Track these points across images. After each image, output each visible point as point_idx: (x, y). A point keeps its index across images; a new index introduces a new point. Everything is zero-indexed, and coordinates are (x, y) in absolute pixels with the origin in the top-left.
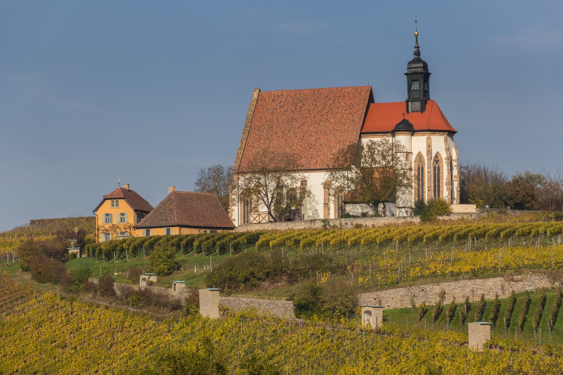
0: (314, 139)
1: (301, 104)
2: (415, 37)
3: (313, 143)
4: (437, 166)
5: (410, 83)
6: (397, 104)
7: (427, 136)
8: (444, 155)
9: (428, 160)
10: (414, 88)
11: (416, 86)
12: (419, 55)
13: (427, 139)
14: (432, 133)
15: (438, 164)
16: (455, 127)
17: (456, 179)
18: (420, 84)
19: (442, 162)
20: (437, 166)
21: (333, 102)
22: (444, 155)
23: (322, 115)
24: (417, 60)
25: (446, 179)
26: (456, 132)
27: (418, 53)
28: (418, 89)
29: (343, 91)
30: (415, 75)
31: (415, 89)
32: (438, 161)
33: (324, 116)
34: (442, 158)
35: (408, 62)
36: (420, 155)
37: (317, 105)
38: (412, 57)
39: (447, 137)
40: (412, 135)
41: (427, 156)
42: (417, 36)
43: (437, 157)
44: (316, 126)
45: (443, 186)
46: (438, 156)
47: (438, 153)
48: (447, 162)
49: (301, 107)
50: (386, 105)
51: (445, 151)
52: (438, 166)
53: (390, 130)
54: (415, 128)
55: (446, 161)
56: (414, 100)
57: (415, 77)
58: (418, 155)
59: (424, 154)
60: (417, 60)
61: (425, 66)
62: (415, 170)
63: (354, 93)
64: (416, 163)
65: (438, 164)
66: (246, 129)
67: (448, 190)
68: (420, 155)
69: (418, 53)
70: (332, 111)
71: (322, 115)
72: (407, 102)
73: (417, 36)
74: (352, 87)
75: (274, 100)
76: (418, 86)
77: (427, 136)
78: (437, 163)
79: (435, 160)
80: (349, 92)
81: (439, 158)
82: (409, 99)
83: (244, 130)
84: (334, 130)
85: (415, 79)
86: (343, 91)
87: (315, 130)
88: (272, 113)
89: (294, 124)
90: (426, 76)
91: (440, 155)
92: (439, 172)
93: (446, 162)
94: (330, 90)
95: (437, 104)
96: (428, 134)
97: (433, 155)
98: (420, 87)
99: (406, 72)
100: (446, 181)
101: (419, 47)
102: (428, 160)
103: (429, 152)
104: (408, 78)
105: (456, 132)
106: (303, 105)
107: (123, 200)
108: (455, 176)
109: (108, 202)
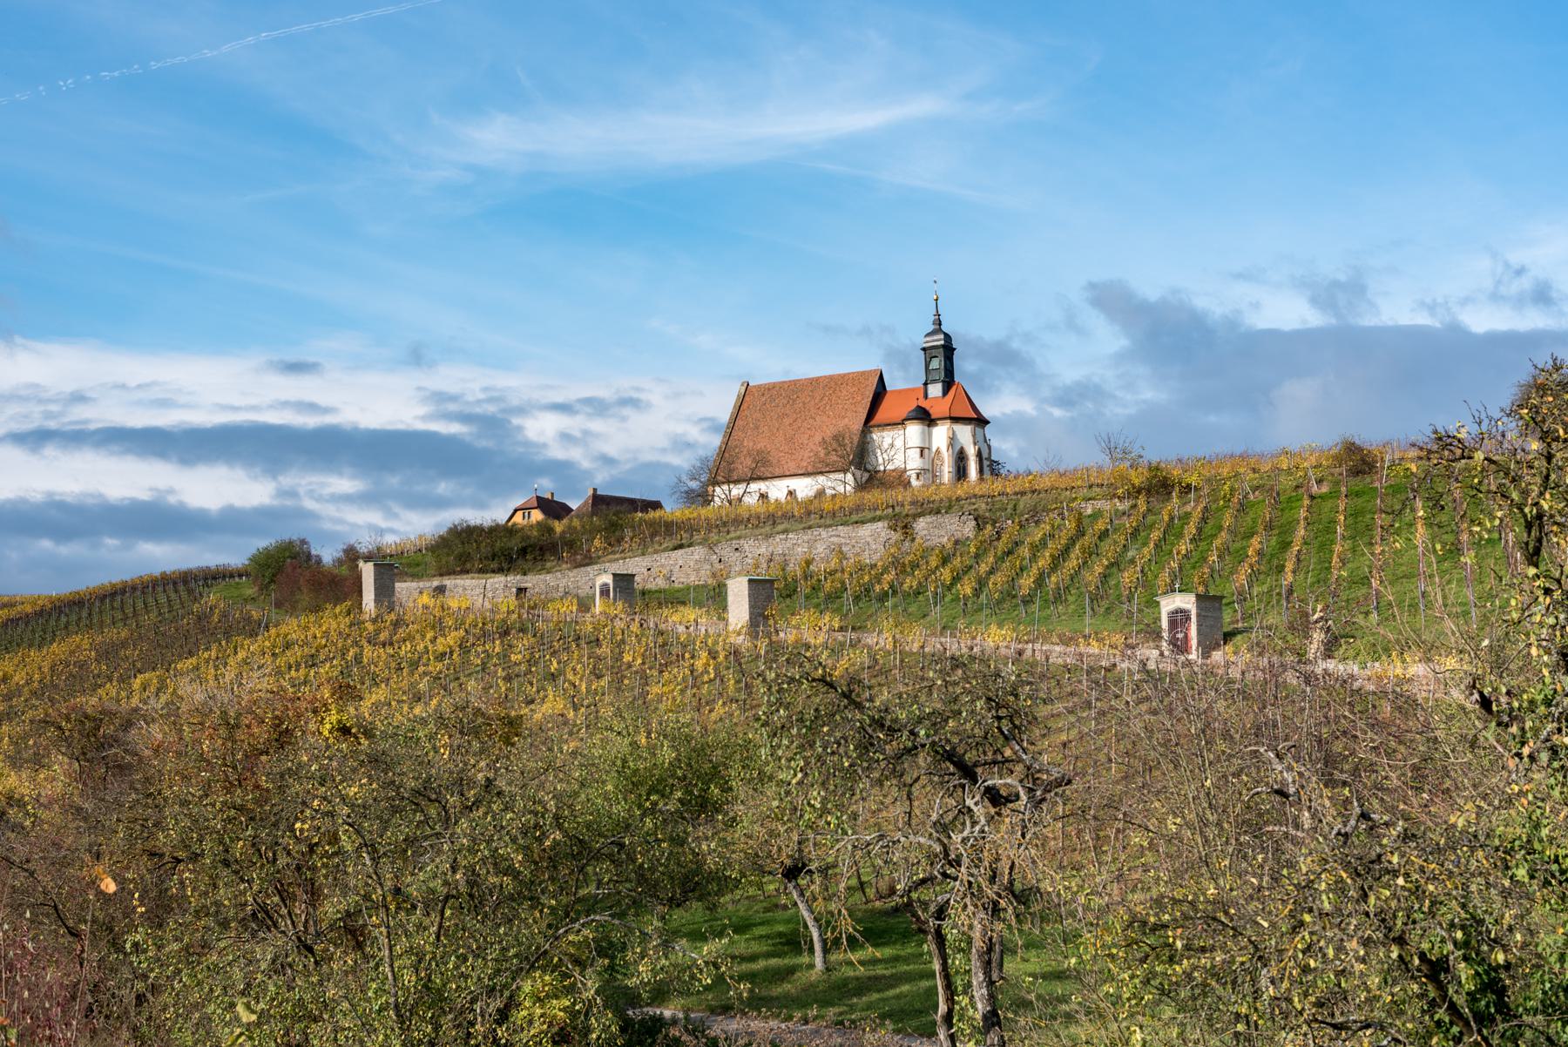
0: (807, 436)
6: (913, 390)
8: (971, 452)
11: (935, 364)
12: (940, 324)
13: (948, 429)
16: (986, 413)
22: (971, 452)
24: (938, 330)
26: (987, 422)
29: (846, 378)
38: (931, 328)
40: (929, 426)
44: (811, 421)
49: (794, 401)
50: (900, 392)
51: (972, 446)
54: (933, 417)
56: (934, 381)
57: (934, 352)
59: (944, 449)
60: (938, 330)
61: (947, 337)
68: (938, 451)
72: (926, 384)
86: (846, 378)
90: (948, 350)
94: (831, 378)
98: (940, 364)
109: (520, 514)
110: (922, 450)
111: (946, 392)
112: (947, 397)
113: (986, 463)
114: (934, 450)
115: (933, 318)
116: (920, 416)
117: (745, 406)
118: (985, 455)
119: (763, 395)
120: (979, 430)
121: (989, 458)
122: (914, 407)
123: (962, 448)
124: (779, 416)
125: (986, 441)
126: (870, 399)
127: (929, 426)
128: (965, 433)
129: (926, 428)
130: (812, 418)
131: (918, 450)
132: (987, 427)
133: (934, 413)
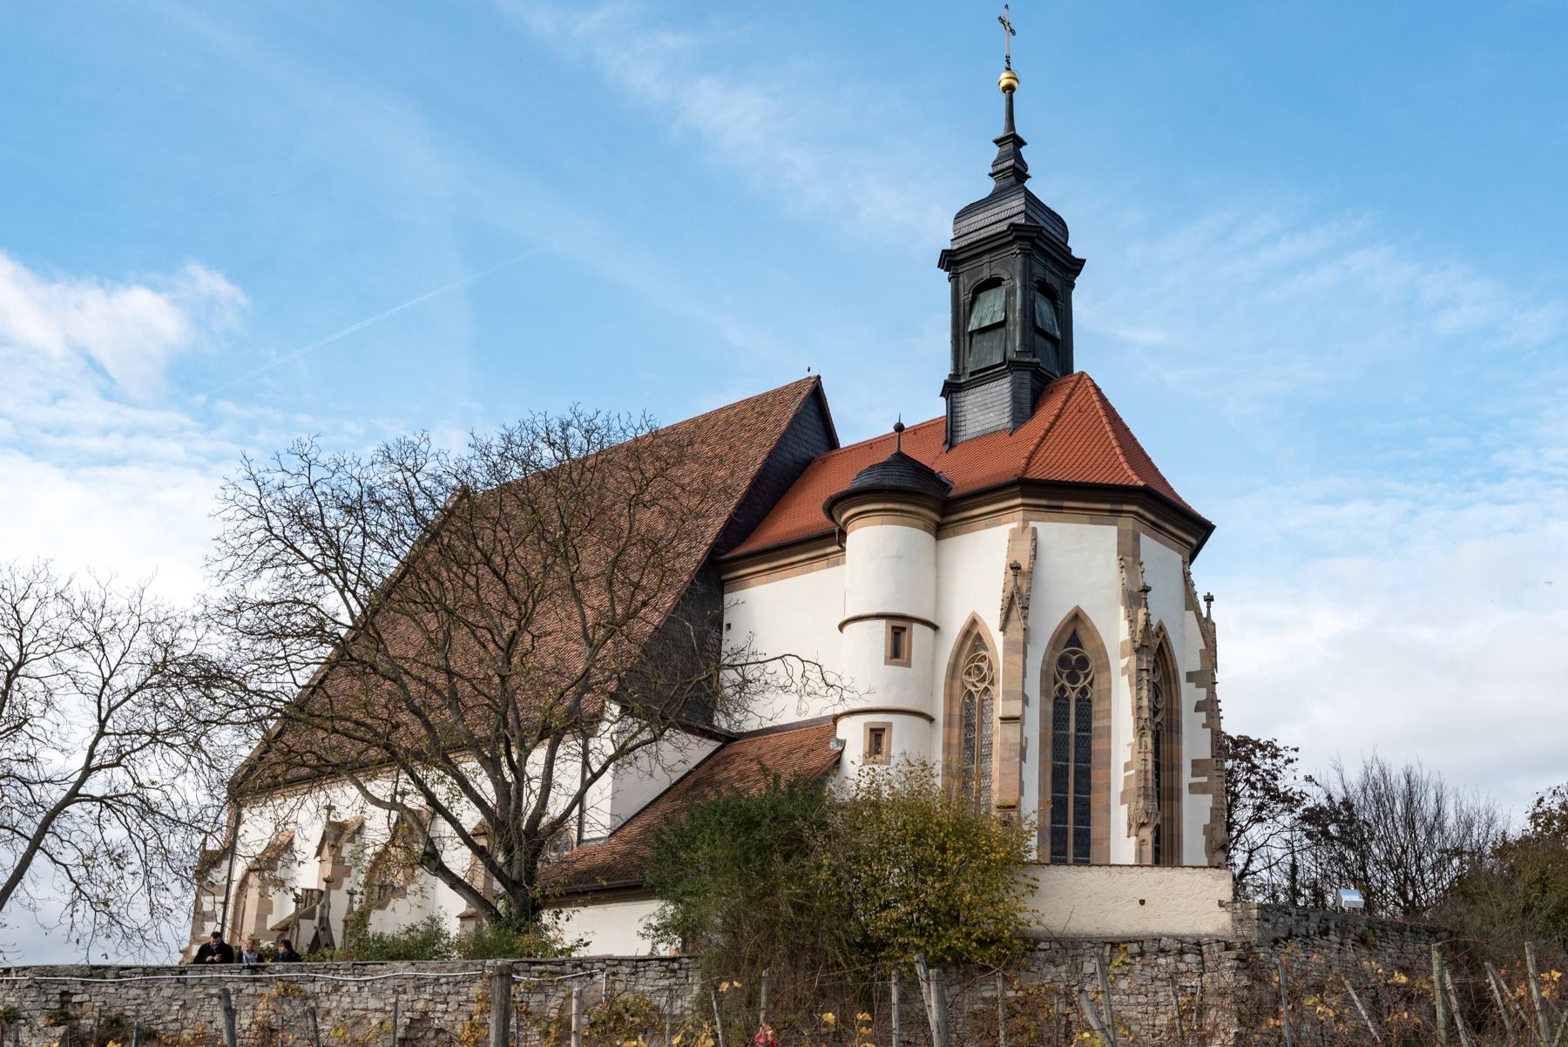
2: (1003, 97)
4: (1073, 696)
5: (962, 297)
7: (1015, 525)
9: (1008, 646)
10: (982, 319)
14: (1044, 502)
15: (1079, 685)
17: (1205, 779)
18: (1010, 293)
19: (1106, 667)
20: (1073, 696)
25: (1127, 767)
27: (1012, 173)
28: (999, 318)
31: (987, 323)
32: (1083, 662)
34: (1101, 650)
35: (958, 211)
36: (972, 636)
39: (1137, 539)
40: (940, 531)
41: (1003, 629)
42: (1010, 89)
43: (1074, 640)
45: (1107, 809)
46: (1082, 634)
47: (1077, 617)
48: (1133, 667)
51: (1122, 609)
52: (1084, 691)
55: (1124, 662)
56: (984, 376)
58: (967, 634)
62: (949, 723)
64: (957, 685)
65: (1079, 685)
67: (1136, 826)
68: (972, 636)
69: (1012, 173)
73: (1010, 89)
77: (1015, 525)
78: (1073, 678)
79: (1063, 662)
81: (1087, 651)
82: (955, 376)
91: (1092, 632)
92: (1089, 730)
93: (1125, 670)
95: (1098, 391)
96: (1019, 514)
97: (1049, 619)
100: (1127, 779)
101: (1019, 143)
102: (1005, 650)
103: (1017, 603)
104: (954, 278)
108: (1196, 764)
110: (899, 628)
111: (1023, 411)
113: (1190, 695)
114: (954, 629)
115: (995, 151)
118: (1187, 659)
120: (1158, 554)
121: (1206, 676)
123: (1077, 617)
125: (1190, 601)
126: (753, 469)
127: (940, 531)
129: (927, 538)
131: (879, 632)
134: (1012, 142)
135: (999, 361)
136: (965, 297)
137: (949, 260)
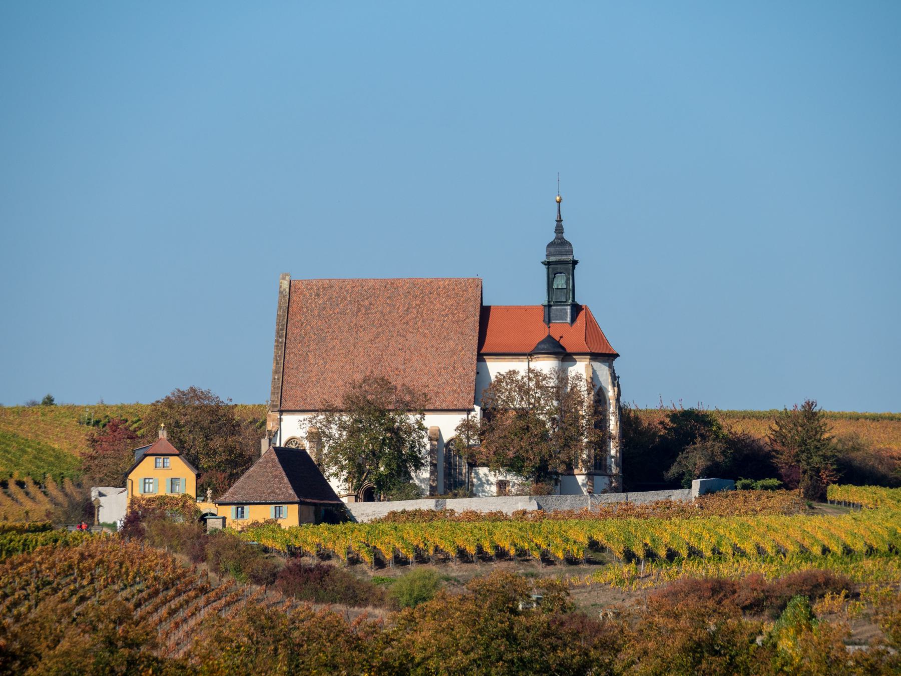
1: (367, 302)
2: (557, 204)
3: (402, 367)
5: (550, 276)
6: (526, 309)
7: (586, 363)
10: (558, 285)
13: (587, 367)
21: (423, 301)
23: (407, 323)
26: (617, 355)
27: (559, 230)
28: (565, 287)
30: (559, 266)
31: (560, 287)
33: (411, 324)
37: (394, 306)
38: (552, 236)
42: (559, 202)
44: (401, 340)
49: (367, 309)
50: (507, 309)
53: (528, 351)
54: (568, 351)
63: (454, 289)
66: (280, 340)
69: (559, 230)
70: (422, 316)
71: (407, 323)
73: (559, 202)
74: (450, 280)
75: (318, 295)
76: (563, 282)
77: (586, 363)
80: (445, 287)
83: (277, 341)
84: (433, 346)
85: (559, 271)
87: (400, 347)
88: (319, 315)
89: (361, 335)
99: (544, 259)
105: (617, 355)
106: (371, 304)
107: (177, 458)
112: (575, 324)
116: (552, 351)
117: (294, 308)
119: (318, 295)
122: (543, 337)
124: (350, 328)
126: (477, 318)
127: (563, 360)
128: (603, 371)
130: (399, 334)
132: (616, 363)
133: (569, 344)
134: (559, 221)
135: (564, 300)
136: (551, 276)
137: (548, 264)
